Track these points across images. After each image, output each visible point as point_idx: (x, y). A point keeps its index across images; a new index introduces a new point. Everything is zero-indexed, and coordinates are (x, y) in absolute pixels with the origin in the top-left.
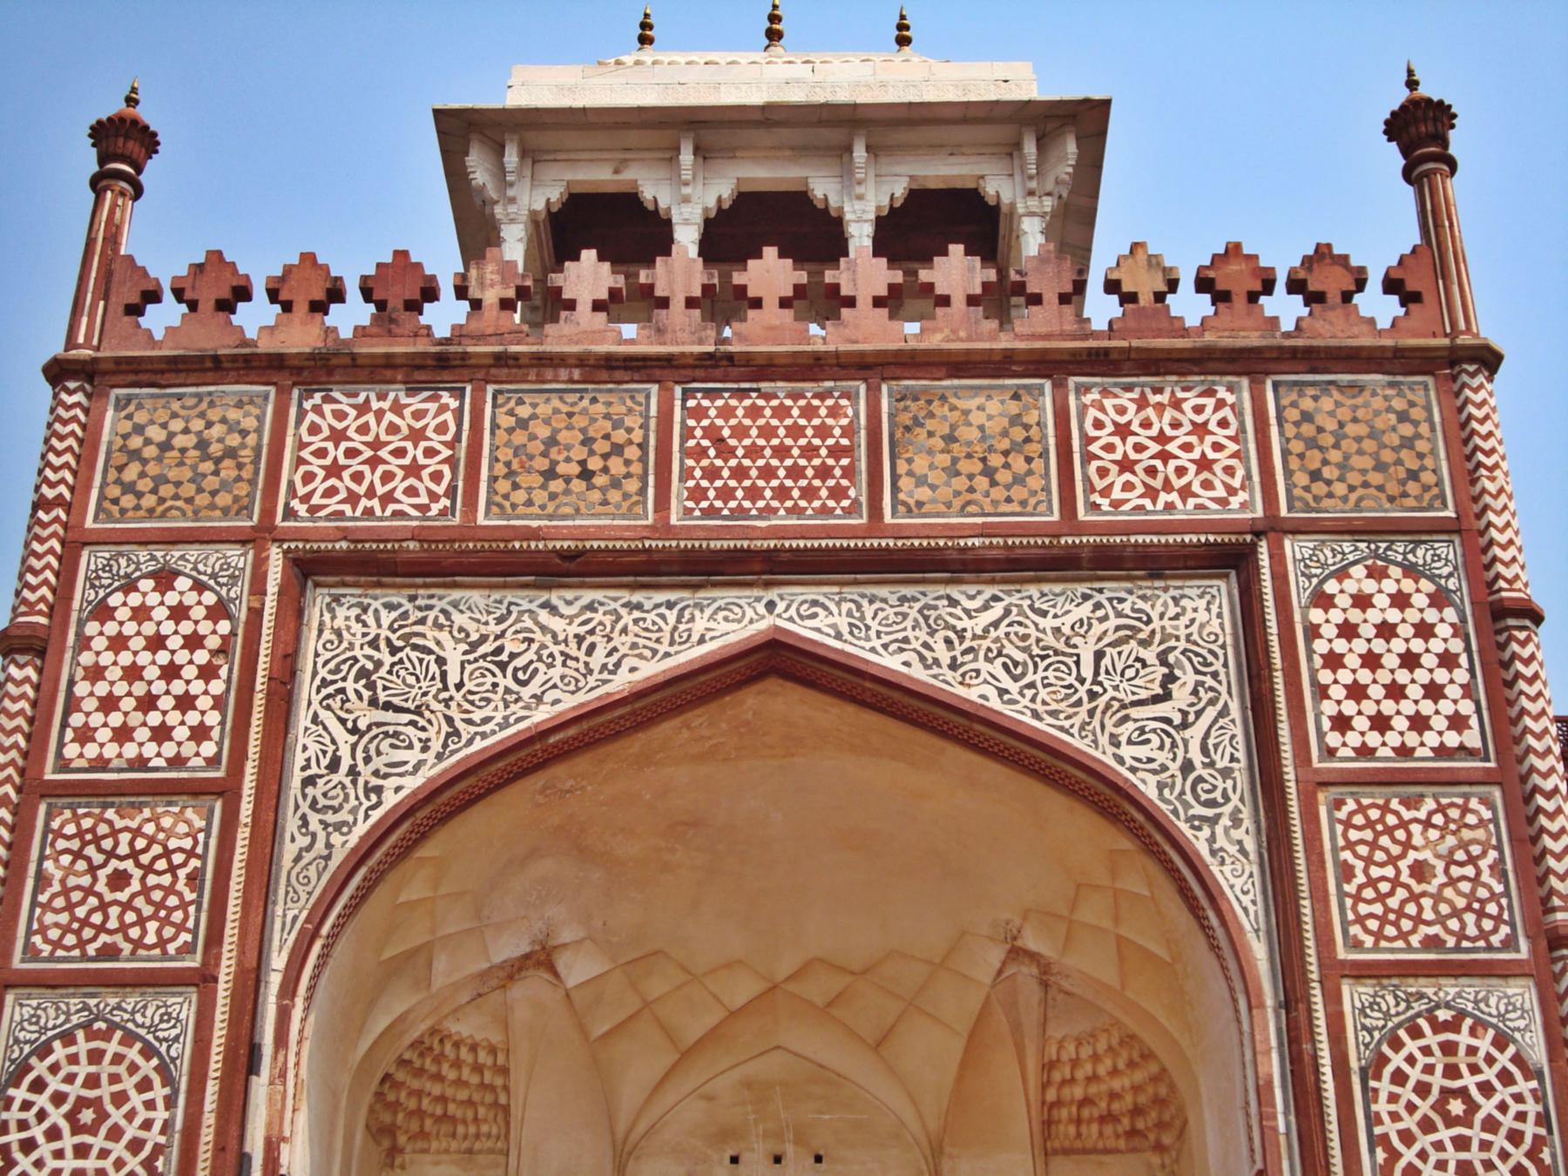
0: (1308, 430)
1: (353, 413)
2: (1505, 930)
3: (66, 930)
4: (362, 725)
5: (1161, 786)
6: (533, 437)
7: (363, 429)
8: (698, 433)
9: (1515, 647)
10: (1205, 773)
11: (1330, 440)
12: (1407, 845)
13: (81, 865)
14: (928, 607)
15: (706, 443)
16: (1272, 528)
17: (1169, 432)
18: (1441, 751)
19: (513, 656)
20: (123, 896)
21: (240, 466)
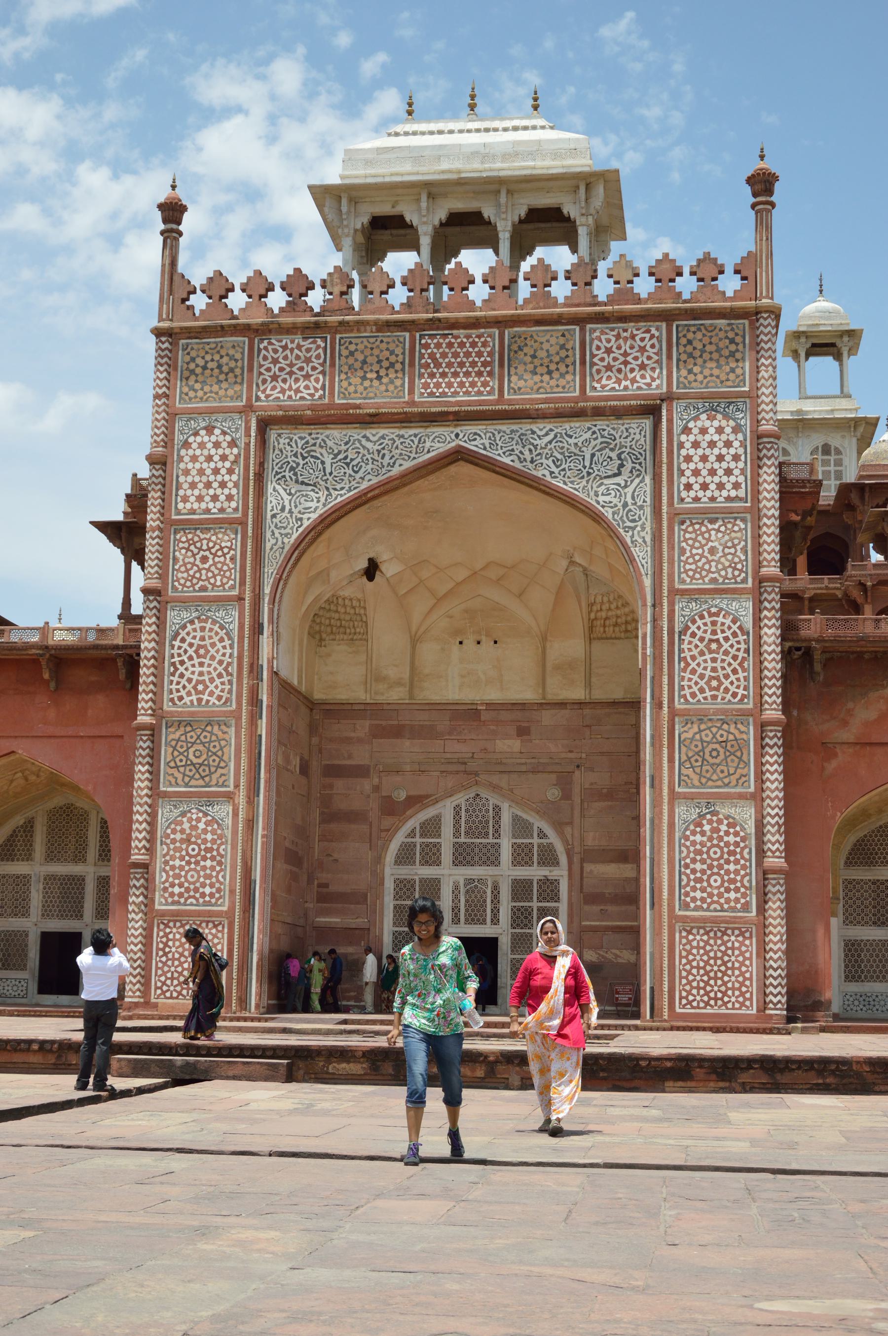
0: (689, 349)
1: (281, 350)
2: (743, 575)
3: (187, 580)
4: (293, 491)
5: (614, 513)
6: (356, 360)
7: (286, 358)
8: (426, 356)
9: (765, 451)
10: (632, 507)
11: (699, 353)
12: (709, 540)
13: (189, 554)
14: (522, 434)
15: (429, 361)
16: (669, 398)
17: (628, 351)
18: (729, 499)
19: (352, 460)
20: (206, 566)
21: (236, 376)
